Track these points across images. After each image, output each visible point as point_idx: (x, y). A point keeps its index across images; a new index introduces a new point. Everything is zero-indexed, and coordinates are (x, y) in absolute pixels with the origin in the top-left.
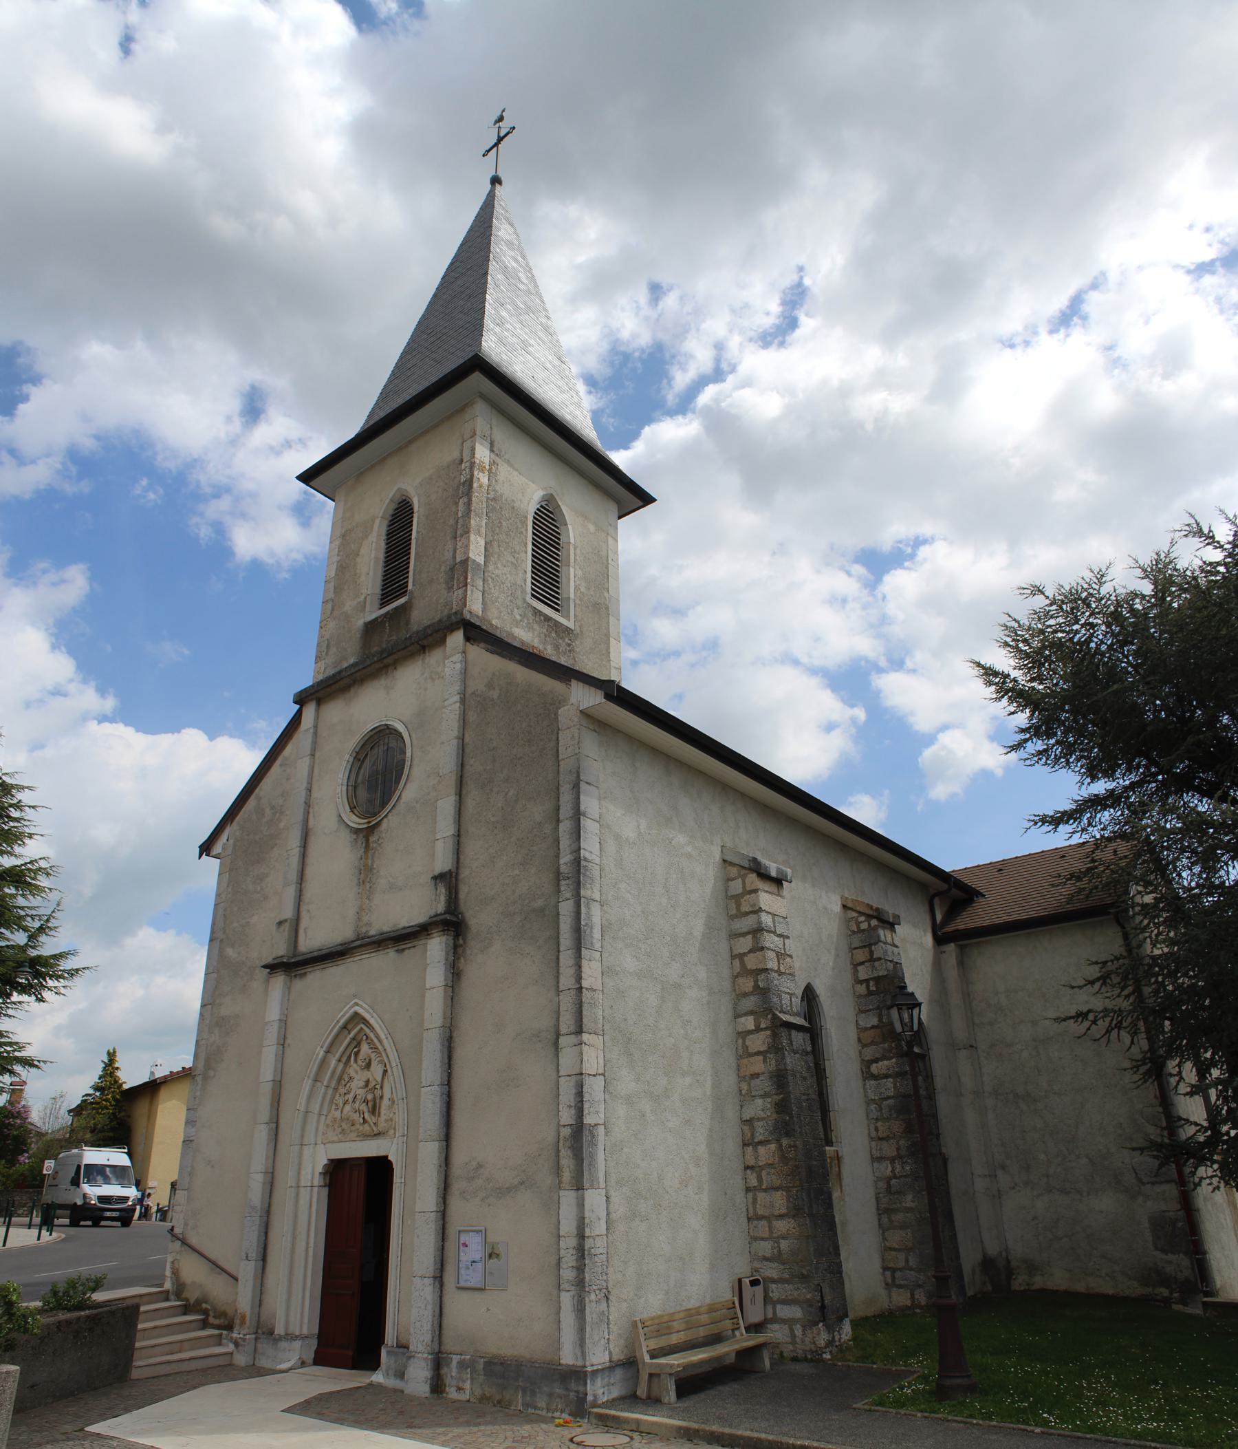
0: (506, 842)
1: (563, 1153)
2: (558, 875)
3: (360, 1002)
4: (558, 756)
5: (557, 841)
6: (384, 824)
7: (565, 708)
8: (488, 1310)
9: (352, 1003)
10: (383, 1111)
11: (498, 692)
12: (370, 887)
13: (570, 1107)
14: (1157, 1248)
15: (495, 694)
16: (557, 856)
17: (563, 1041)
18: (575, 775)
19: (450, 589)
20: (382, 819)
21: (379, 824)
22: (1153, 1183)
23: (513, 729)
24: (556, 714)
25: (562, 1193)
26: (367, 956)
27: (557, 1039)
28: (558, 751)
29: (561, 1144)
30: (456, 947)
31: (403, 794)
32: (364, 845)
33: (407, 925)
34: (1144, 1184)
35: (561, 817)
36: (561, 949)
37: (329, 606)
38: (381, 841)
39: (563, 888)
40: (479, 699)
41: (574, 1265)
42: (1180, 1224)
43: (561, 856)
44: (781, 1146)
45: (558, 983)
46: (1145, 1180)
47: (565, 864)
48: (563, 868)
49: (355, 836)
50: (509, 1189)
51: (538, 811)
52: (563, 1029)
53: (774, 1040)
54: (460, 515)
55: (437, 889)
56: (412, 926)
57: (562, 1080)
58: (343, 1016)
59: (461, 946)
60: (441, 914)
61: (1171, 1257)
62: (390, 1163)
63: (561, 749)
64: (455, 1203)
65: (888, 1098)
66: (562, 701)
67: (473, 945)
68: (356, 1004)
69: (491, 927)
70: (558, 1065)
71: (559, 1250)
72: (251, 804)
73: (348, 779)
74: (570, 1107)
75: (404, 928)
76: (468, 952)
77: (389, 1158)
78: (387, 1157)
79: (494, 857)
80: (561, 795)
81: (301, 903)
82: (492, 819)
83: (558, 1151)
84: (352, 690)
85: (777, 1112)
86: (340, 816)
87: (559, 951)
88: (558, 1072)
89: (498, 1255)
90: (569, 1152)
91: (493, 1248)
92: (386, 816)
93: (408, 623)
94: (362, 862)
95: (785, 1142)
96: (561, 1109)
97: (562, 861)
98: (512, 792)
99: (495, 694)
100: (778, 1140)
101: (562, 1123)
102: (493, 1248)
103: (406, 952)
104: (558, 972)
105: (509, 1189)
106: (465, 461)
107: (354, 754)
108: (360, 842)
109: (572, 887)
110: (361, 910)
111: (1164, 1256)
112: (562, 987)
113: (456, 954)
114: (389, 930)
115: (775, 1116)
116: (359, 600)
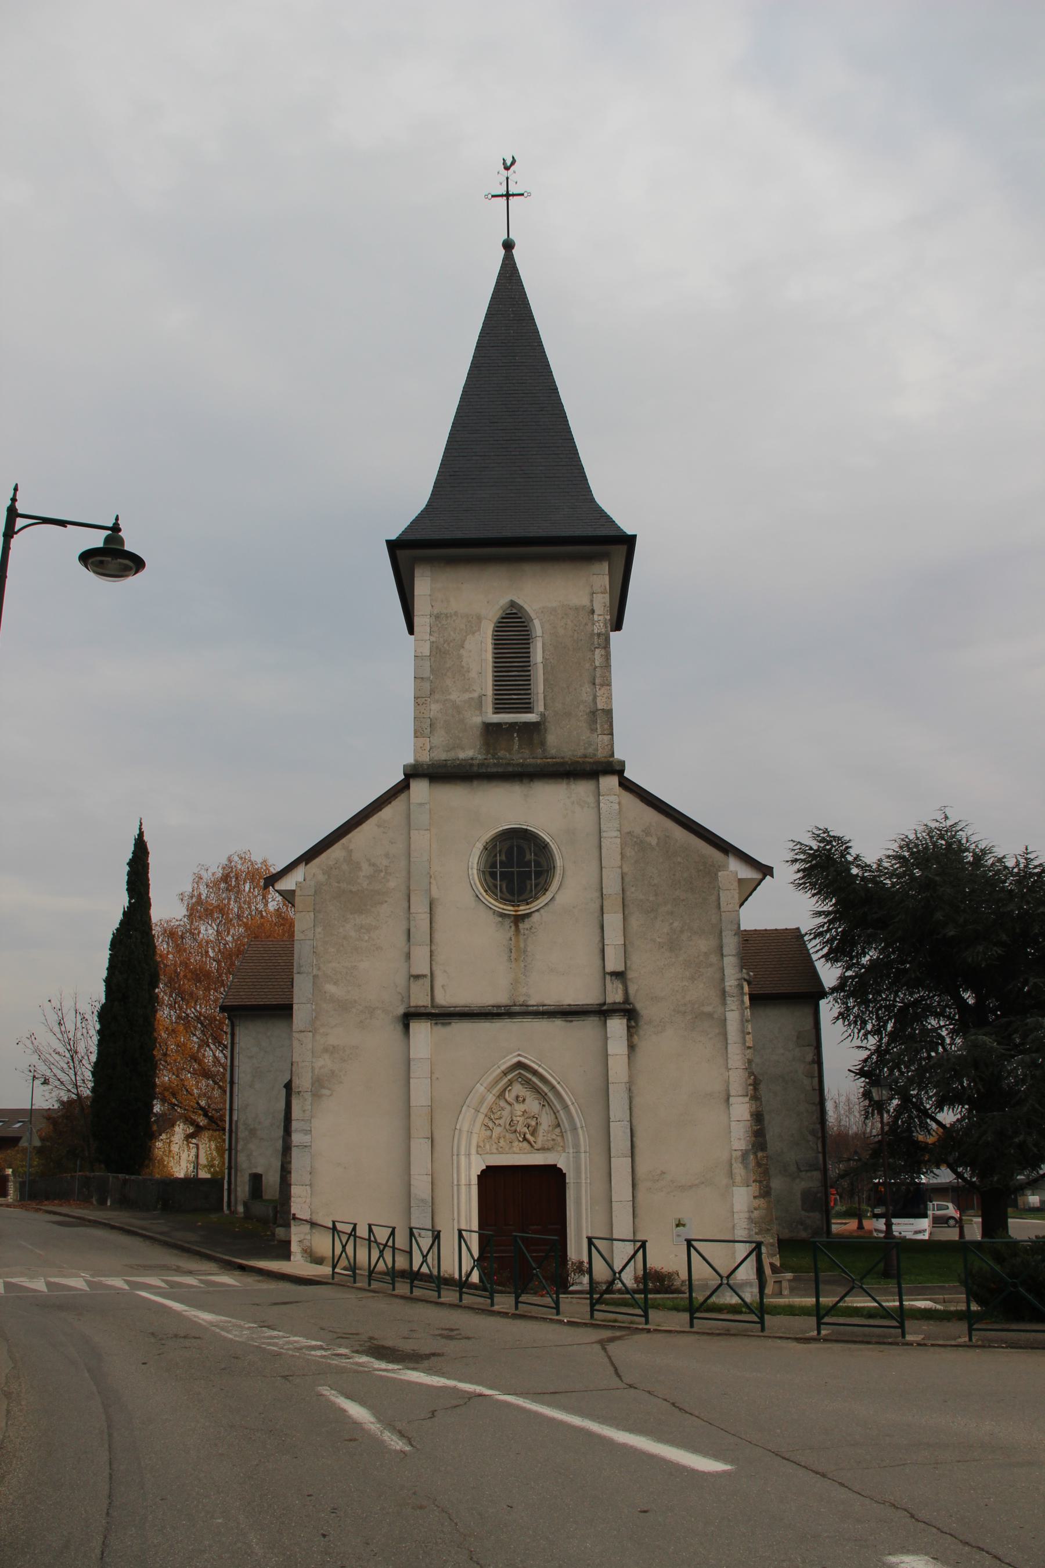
0: (673, 960)
1: (735, 1165)
2: (723, 994)
3: (523, 1054)
4: (720, 908)
5: (722, 970)
6: (536, 917)
7: (725, 872)
8: (676, 1256)
9: (517, 1053)
10: (541, 1134)
11: (656, 840)
12: (525, 966)
13: (740, 1139)
14: (803, 1209)
15: (654, 841)
16: (723, 979)
17: (732, 1100)
18: (736, 926)
19: (593, 730)
20: (534, 912)
21: (529, 915)
22: (807, 1171)
23: (674, 875)
24: (716, 874)
25: (734, 1188)
26: (529, 1020)
27: (728, 1099)
28: (719, 904)
29: (733, 1161)
30: (629, 1027)
31: (557, 897)
32: (513, 928)
33: (572, 1003)
34: (801, 1171)
35: (725, 952)
36: (729, 1042)
37: (427, 686)
38: (533, 930)
39: (728, 1002)
40: (635, 840)
41: (746, 1227)
42: (819, 1195)
43: (726, 980)
44: (757, 1156)
45: (727, 1063)
46: (802, 1169)
47: (731, 986)
48: (727, 989)
49: (500, 919)
50: (691, 1187)
51: (704, 944)
52: (732, 1092)
53: (755, 1093)
54: (597, 664)
55: (613, 984)
56: (579, 1005)
57: (733, 1124)
58: (505, 1063)
59: (634, 1027)
60: (619, 1003)
61: (811, 1214)
62: (560, 1170)
63: (723, 904)
64: (640, 1196)
65: (167, 1051)
66: (724, 867)
67: (645, 1030)
68: (519, 1055)
69: (663, 1018)
70: (729, 1114)
71: (734, 1219)
72: (336, 852)
73: (478, 863)
74: (740, 1139)
75: (569, 1005)
76: (641, 1032)
77: (558, 1166)
78: (556, 1165)
79: (663, 969)
80: (724, 937)
81: (433, 963)
82: (658, 940)
83: (731, 1165)
84: (475, 783)
85: (755, 1136)
86: (477, 896)
87: (727, 1043)
88: (730, 1118)
89: (684, 1225)
90: (740, 1165)
91: (679, 1221)
92: (537, 910)
93: (543, 743)
94: (512, 942)
95: (760, 1154)
96: (732, 1140)
97: (727, 984)
98: (676, 924)
99: (654, 841)
100: (755, 1154)
101: (734, 1148)
102: (679, 1221)
103: (574, 1023)
104: (727, 1056)
105: (691, 1187)
106: (597, 612)
107: (485, 844)
108: (507, 927)
109: (737, 1003)
110: (515, 983)
111: (807, 1214)
112: (730, 1066)
113: (631, 1031)
114: (552, 1004)
115: (753, 1139)
116: (471, 696)
